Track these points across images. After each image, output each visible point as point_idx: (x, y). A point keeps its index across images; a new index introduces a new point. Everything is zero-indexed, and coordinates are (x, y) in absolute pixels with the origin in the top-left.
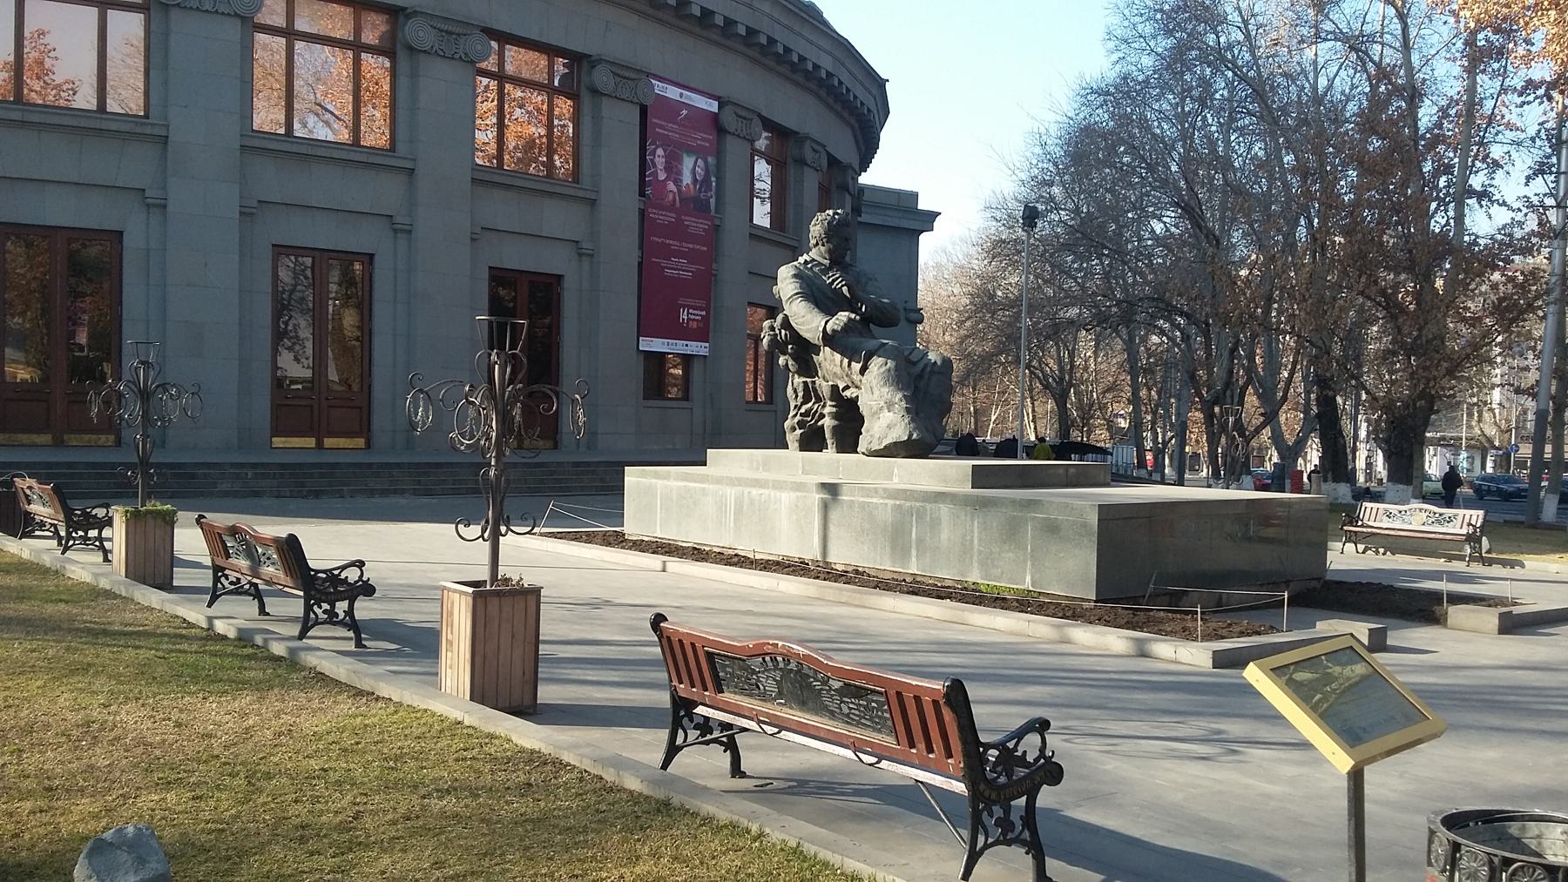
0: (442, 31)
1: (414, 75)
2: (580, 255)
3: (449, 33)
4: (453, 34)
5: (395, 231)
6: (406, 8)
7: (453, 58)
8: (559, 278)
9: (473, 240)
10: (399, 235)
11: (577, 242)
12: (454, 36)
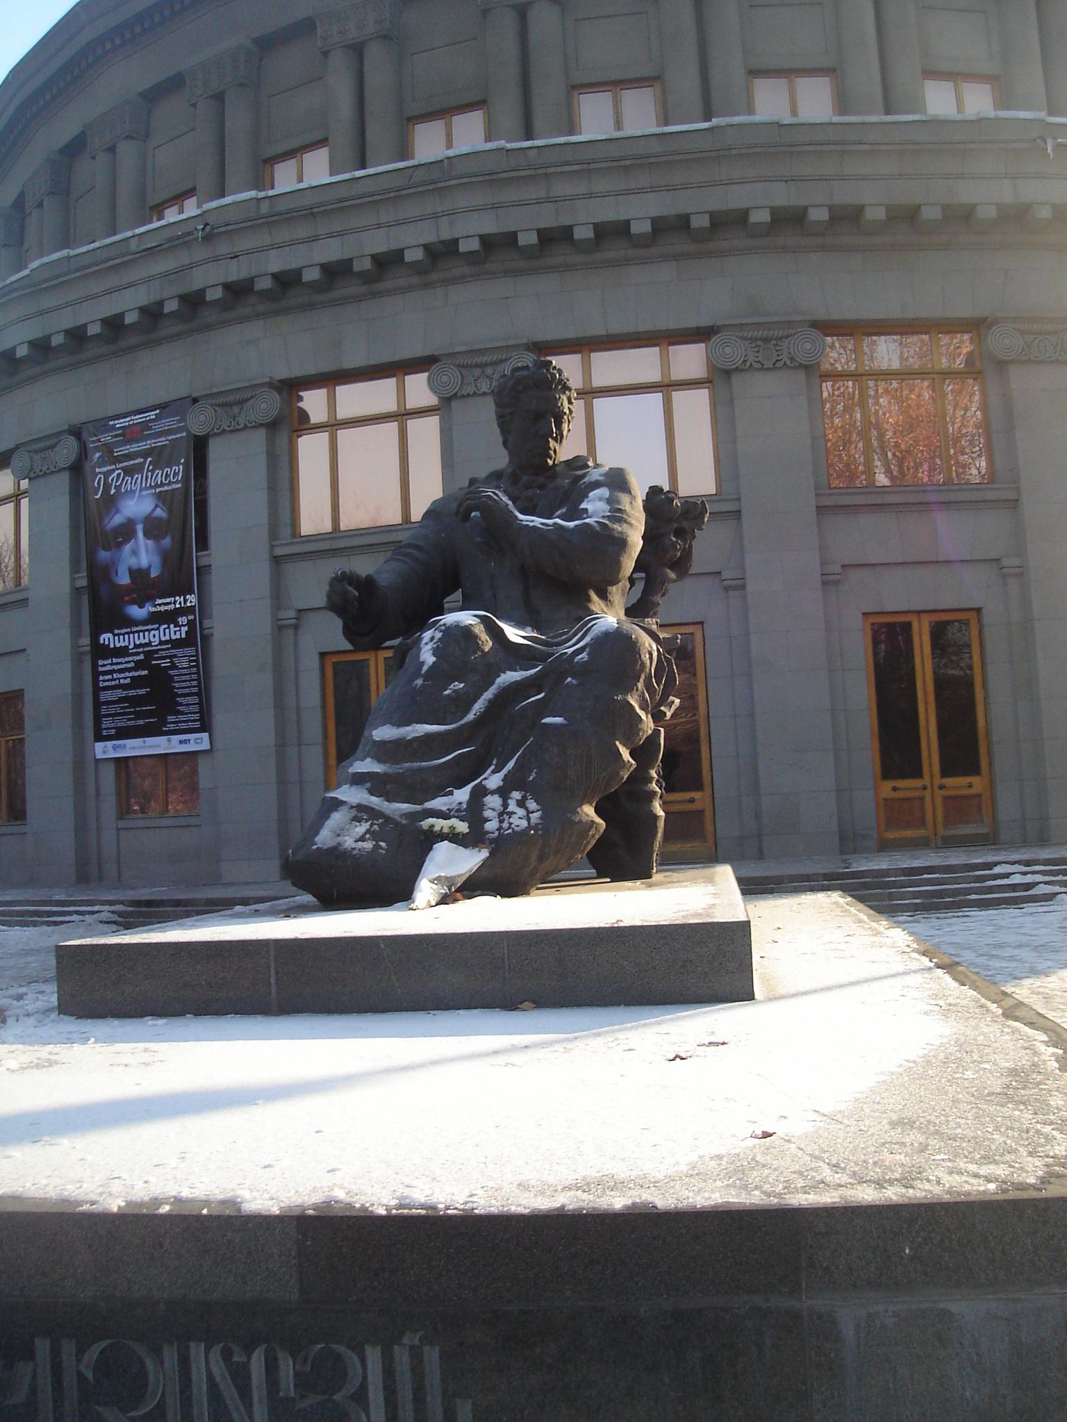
0: (756, 340)
1: (731, 402)
2: (1004, 577)
3: (766, 340)
4: (771, 339)
5: (726, 589)
6: (713, 326)
7: (774, 368)
8: (978, 610)
9: (824, 583)
10: (731, 593)
11: (998, 560)
12: (774, 342)
